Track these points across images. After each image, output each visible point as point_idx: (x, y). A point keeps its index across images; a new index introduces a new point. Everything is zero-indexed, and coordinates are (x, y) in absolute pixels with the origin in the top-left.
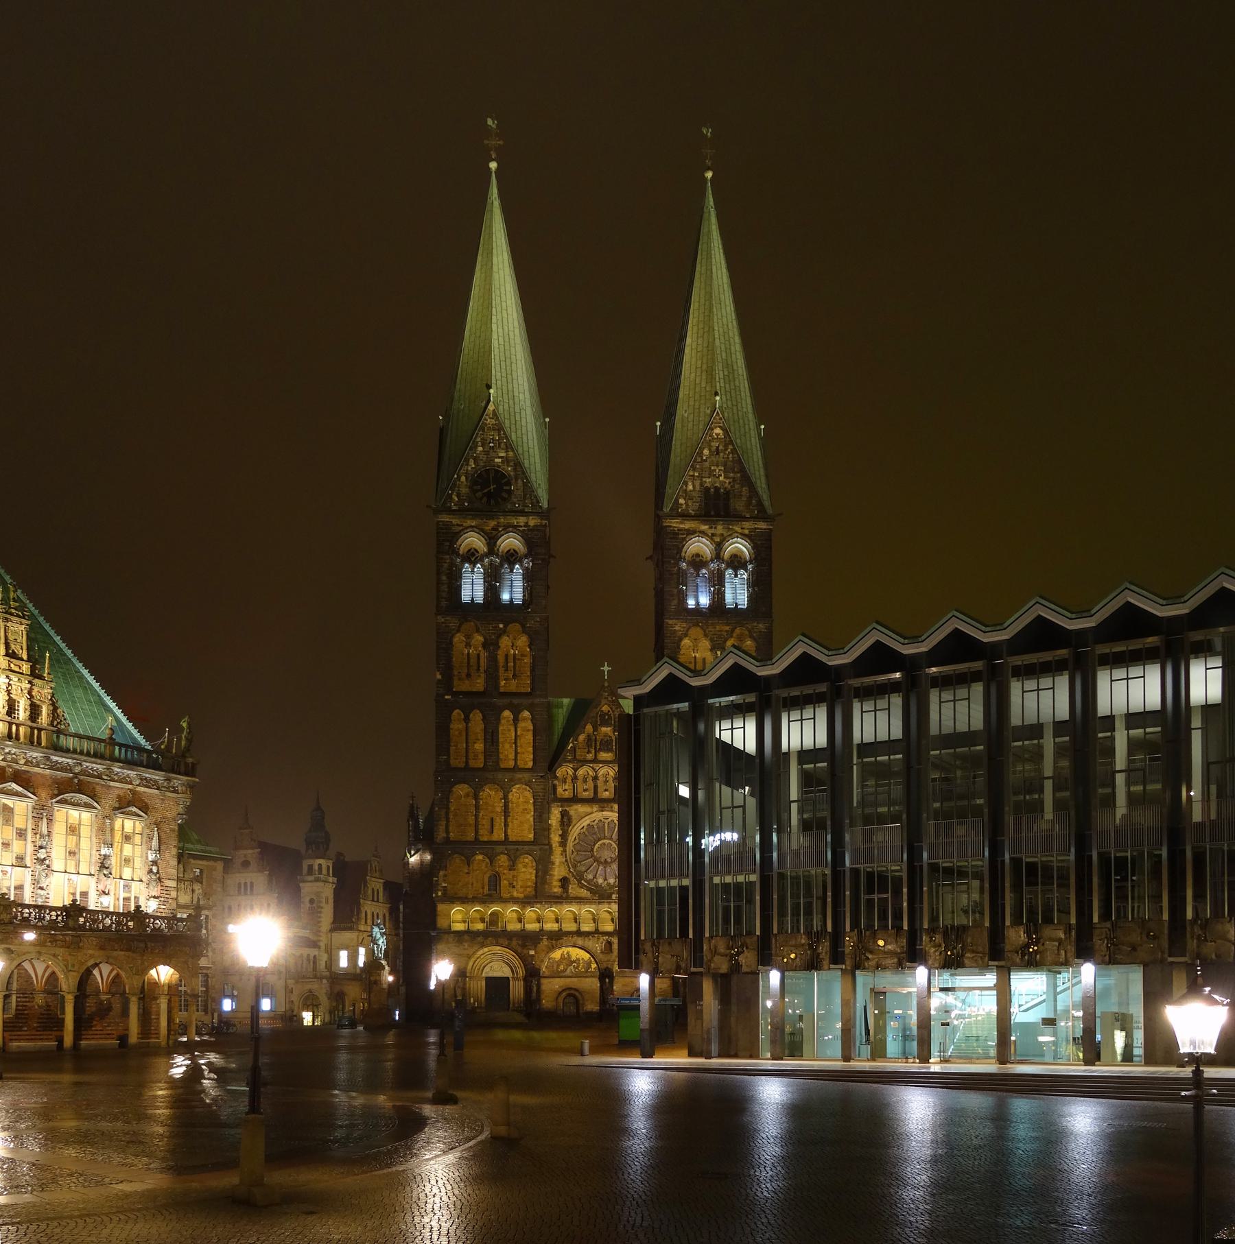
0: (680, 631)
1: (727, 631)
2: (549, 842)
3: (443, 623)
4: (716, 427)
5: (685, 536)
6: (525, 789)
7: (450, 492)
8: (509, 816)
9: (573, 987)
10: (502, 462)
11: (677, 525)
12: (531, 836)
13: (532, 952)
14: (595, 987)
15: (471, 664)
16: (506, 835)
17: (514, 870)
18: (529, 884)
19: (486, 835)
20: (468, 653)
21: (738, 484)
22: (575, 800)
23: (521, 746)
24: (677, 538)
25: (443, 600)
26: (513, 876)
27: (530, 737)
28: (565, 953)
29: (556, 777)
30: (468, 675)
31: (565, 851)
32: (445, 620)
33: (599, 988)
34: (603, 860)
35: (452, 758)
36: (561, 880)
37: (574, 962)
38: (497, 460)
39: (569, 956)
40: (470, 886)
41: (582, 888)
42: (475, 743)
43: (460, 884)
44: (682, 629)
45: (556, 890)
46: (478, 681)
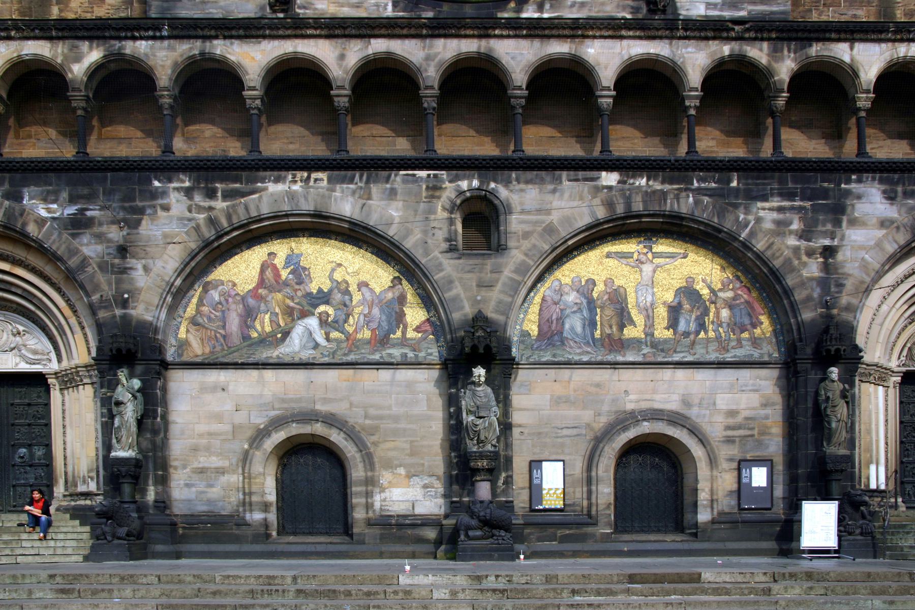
37: (323, 297)
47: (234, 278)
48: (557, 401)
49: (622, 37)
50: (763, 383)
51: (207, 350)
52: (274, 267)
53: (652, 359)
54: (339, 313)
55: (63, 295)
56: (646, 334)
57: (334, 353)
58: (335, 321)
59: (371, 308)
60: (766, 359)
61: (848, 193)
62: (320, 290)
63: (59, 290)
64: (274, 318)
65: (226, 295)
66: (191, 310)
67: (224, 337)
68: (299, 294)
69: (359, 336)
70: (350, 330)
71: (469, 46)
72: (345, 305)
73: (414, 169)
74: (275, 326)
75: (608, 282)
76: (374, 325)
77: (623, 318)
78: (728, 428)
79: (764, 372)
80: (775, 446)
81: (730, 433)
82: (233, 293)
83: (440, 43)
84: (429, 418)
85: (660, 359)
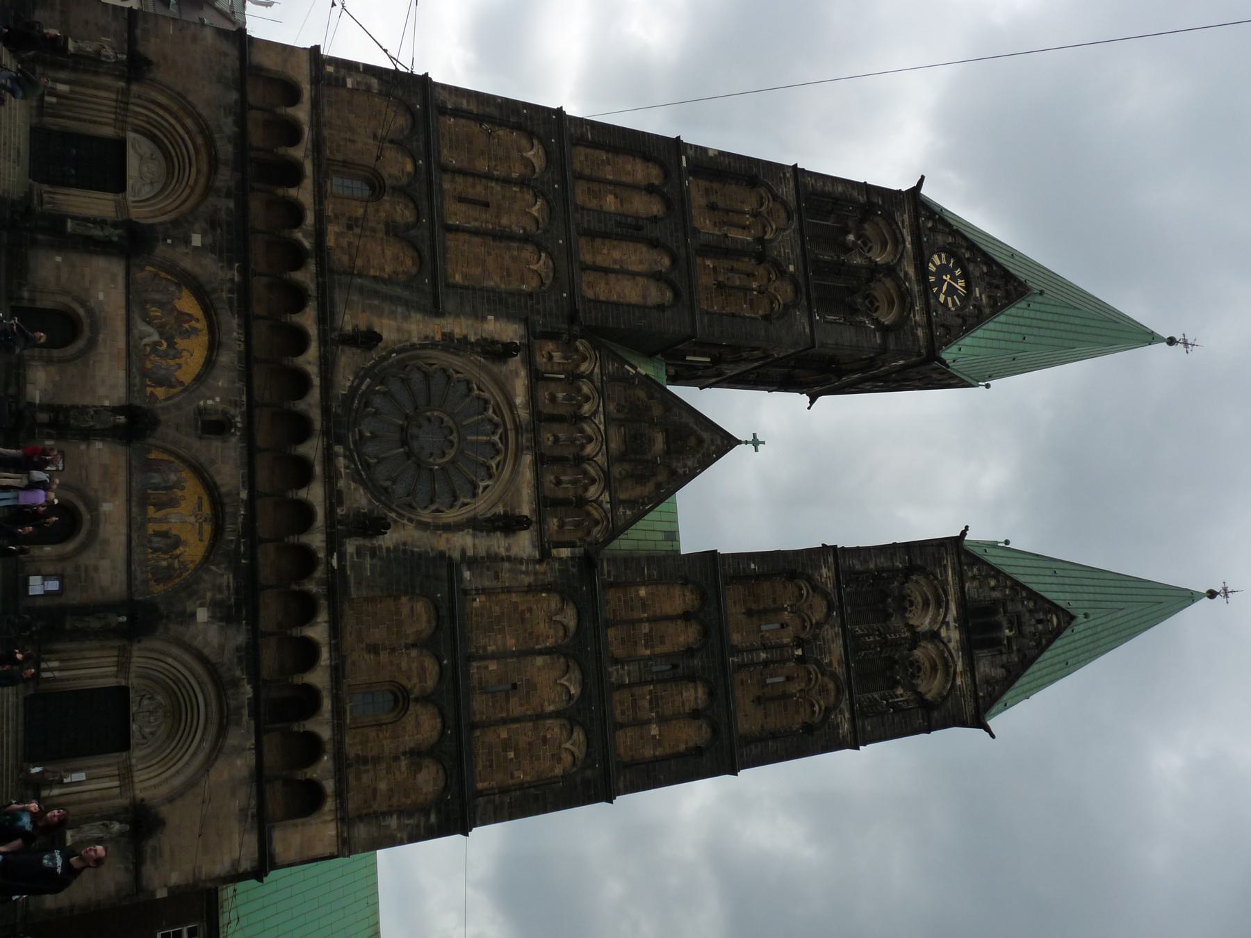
0: (821, 576)
1: (831, 662)
3: (785, 175)
4: (1058, 618)
5: (940, 578)
7: (937, 216)
9: (101, 336)
10: (976, 298)
11: (949, 564)
12: (458, 278)
13: (196, 240)
14: (101, 391)
15: (730, 214)
16: (456, 229)
17: (387, 233)
18: (359, 262)
19: (455, 189)
20: (745, 213)
21: (1008, 659)
22: (536, 377)
24: (935, 565)
25: (813, 181)
26: (374, 230)
29: (575, 338)
30: (712, 207)
32: (788, 180)
34: (414, 431)
35: (588, 150)
37: (171, 345)
38: (977, 290)
39: (187, 334)
40: (348, 136)
41: (356, 376)
42: (616, 197)
43: (352, 117)
44: (823, 580)
45: (347, 317)
46: (707, 222)
49: (325, 501)
55: (173, 210)
56: (149, 519)
58: (157, 350)
62: (176, 343)
63: (177, 208)
66: (163, 274)
68: (174, 332)
69: (148, 362)
70: (152, 357)
71: (318, 425)
72: (167, 356)
73: (247, 394)
75: (184, 498)
77: (160, 506)
78: (86, 568)
79: (125, 587)
80: (75, 597)
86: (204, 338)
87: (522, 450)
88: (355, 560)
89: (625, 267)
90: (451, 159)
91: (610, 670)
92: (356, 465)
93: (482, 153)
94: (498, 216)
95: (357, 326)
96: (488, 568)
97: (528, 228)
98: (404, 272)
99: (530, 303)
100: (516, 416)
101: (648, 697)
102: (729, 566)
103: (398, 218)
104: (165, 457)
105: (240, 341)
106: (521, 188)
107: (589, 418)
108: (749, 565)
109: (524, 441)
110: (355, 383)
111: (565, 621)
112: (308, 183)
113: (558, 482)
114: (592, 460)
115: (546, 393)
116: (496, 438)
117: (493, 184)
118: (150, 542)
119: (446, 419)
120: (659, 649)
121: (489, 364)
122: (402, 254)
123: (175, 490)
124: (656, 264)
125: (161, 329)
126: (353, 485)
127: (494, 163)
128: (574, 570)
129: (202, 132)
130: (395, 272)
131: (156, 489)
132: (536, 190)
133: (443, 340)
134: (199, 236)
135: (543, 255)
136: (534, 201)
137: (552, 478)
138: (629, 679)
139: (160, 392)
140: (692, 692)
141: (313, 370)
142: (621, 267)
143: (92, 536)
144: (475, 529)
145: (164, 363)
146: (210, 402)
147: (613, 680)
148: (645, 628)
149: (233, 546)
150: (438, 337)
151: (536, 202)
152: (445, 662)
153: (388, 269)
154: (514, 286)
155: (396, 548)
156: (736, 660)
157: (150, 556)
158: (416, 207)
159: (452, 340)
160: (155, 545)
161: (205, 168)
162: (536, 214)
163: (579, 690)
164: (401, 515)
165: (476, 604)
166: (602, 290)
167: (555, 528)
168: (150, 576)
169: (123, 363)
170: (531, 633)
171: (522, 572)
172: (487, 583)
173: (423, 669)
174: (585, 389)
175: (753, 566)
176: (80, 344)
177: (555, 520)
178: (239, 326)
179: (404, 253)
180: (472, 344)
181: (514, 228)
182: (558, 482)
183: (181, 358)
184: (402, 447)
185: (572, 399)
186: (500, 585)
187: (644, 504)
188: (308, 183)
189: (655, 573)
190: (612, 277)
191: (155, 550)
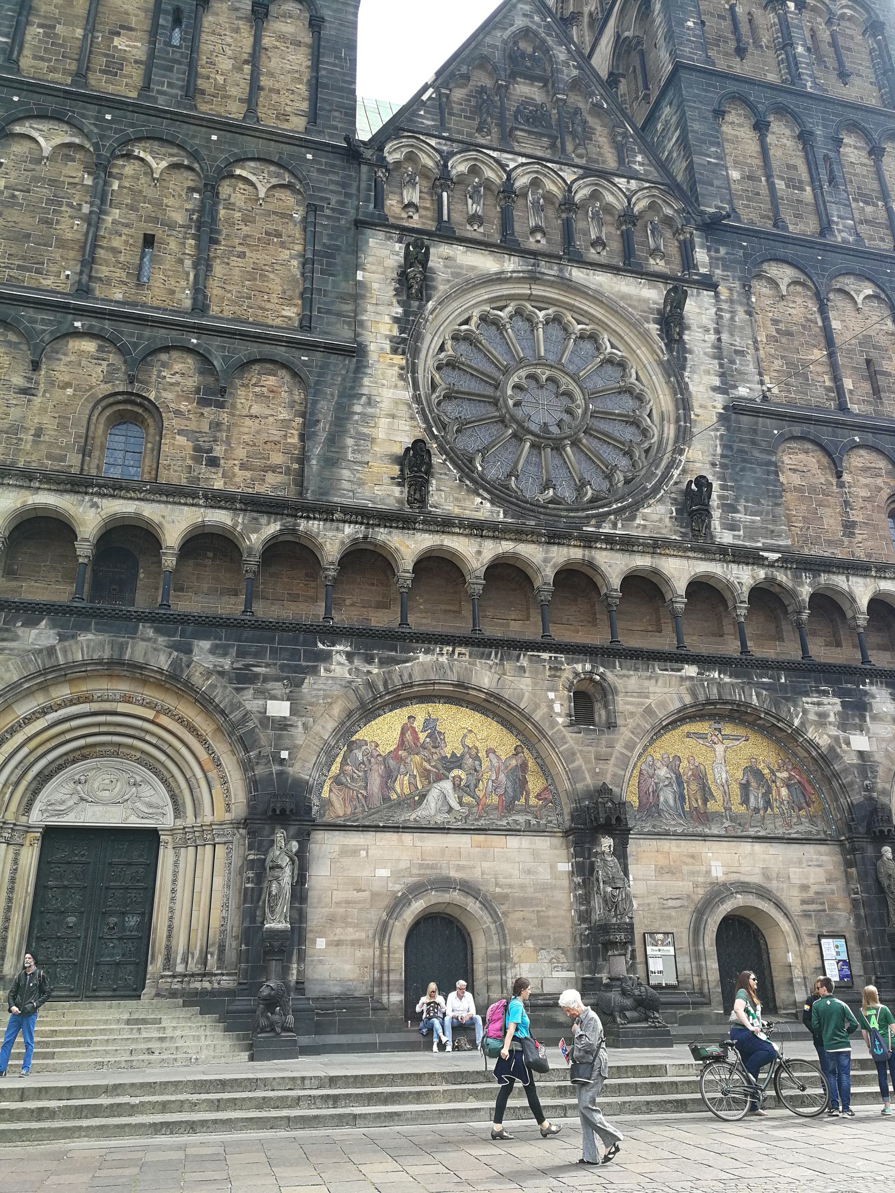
2: (357, 335)
6: (278, 176)
8: (216, 242)
9: (453, 874)
12: (292, 312)
13: (279, 709)
14: (544, 875)
17: (221, 405)
18: (277, 458)
23: (271, 75)
26: (216, 425)
27: (299, 60)
28: (418, 724)
31: (414, 371)
33: (565, 883)
35: (26, 52)
36: (399, 460)
37: (455, 762)
39: (436, 737)
42: (118, 34)
45: (378, 491)
47: (376, 739)
48: (661, 871)
49: (689, 557)
50: (824, 858)
51: (349, 811)
52: (414, 732)
53: (733, 834)
54: (470, 777)
55: (208, 748)
57: (466, 817)
59: (497, 774)
60: (822, 836)
61: (866, 693)
62: (453, 755)
63: (204, 742)
64: (412, 780)
65: (369, 755)
66: (335, 768)
67: (365, 798)
68: (435, 757)
69: (488, 801)
70: (480, 794)
71: (576, 553)
72: (476, 770)
74: (412, 788)
76: (501, 791)
77: (706, 794)
78: (803, 902)
79: (823, 848)
80: (844, 919)
81: (806, 907)
82: (376, 754)
83: (555, 548)
84: (553, 887)
85: (740, 834)
86: (442, 712)
87: (562, 278)
88: (741, 533)
89: (245, 56)
90: (62, 277)
91: (840, 239)
92: (609, 513)
93: (48, 222)
94: (171, 225)
95: (393, 478)
96: (732, 362)
97: (191, 184)
98: (291, 392)
99: (328, 212)
100: (515, 275)
101: (861, 204)
102: (696, 54)
103: (192, 382)
104: (635, 781)
105: (453, 651)
106: (111, 175)
107: (509, 174)
108: (689, 28)
109: (552, 273)
110: (486, 495)
111: (787, 280)
112: (150, 511)
113: (598, 242)
114: (570, 187)
115: (469, 227)
116: (541, 315)
117: (109, 219)
118: (757, 810)
119: (514, 379)
120: (805, 176)
121: (437, 296)
122: (257, 389)
123: (681, 771)
124: (237, 9)
125: (432, 777)
126: (639, 521)
127: (64, 208)
128: (723, 251)
129: (43, 687)
130: (292, 404)
131: (682, 797)
132: (117, 153)
133: (404, 353)
134: (269, 702)
135: (238, 172)
136: (136, 162)
137: (593, 251)
138: (847, 219)
139: (535, 784)
140: (848, 150)
141: (491, 549)
142: (246, 62)
143: (763, 893)
144: (683, 368)
145: (488, 776)
146: (557, 708)
147: (851, 239)
148: (780, 184)
149: (764, 692)
150: (399, 360)
151: (142, 160)
152: (857, 439)
153: (284, 415)
154: (297, 232)
155: (723, 478)
156: (809, 84)
157: (776, 810)
158: (166, 349)
159: (404, 340)
160: (761, 804)
161: (123, 687)
162: (164, 164)
163: (867, 283)
164: (672, 465)
165: (775, 391)
166: (290, 103)
167: (662, 263)
168: (802, 813)
169: (496, 841)
170: (803, 326)
171: (732, 319)
172: (751, 368)
173: (865, 469)
174: (463, 168)
175: (690, 24)
176: (473, 906)
177: (652, 261)
178: (427, 652)
179: (255, 385)
180: (406, 313)
181: (189, 206)
182: (598, 242)
183: (477, 748)
184: (564, 447)
185: (476, 189)
186: (751, 351)
187: (625, 135)
188: (150, 511)
189: (713, 149)
190: (264, 81)
191: (768, 804)
